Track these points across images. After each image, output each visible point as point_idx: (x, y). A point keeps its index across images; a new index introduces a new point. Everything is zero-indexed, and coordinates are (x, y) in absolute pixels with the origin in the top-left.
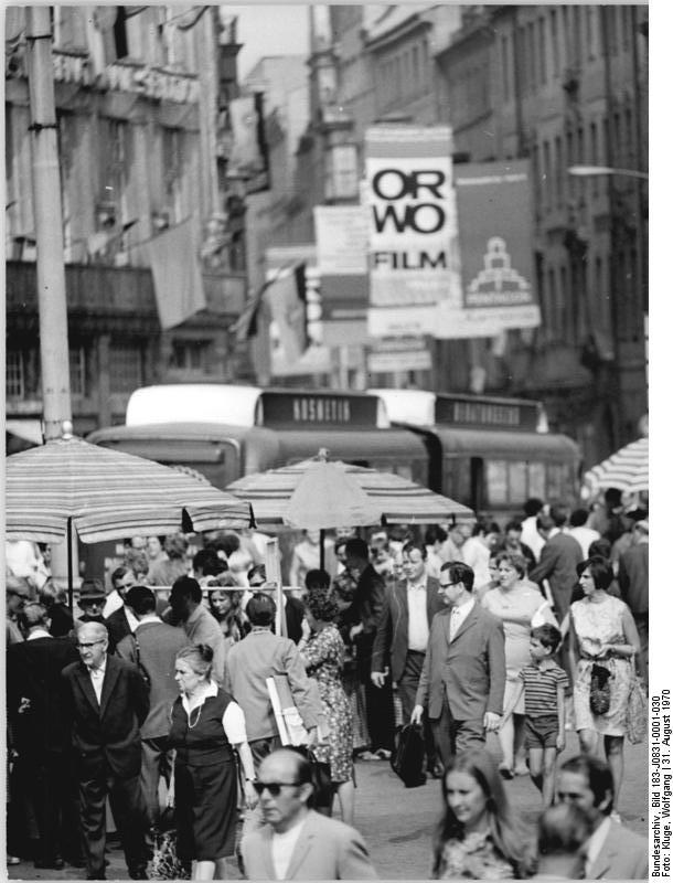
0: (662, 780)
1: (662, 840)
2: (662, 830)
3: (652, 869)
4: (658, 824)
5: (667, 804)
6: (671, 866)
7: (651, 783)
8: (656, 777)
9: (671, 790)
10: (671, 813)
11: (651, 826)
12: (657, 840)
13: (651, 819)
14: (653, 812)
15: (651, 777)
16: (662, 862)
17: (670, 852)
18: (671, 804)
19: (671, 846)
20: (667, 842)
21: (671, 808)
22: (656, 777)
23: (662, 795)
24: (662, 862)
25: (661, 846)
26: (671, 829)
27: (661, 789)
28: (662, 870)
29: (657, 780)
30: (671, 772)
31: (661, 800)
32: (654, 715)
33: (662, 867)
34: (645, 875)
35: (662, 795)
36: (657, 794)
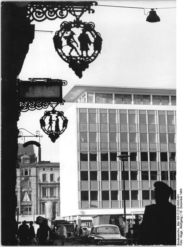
0: (180, 218)
1: (180, 235)
2: (180, 232)
3: (177, 243)
4: (179, 230)
5: (181, 225)
6: (182, 242)
7: (177, 219)
9: (182, 221)
10: (182, 227)
11: (177, 231)
12: (179, 235)
13: (177, 229)
14: (177, 227)
15: (177, 218)
16: (180, 241)
19: (182, 237)
20: (181, 235)
21: (182, 226)
23: (180, 222)
24: (180, 241)
25: (180, 237)
27: (180, 221)
29: (178, 218)
30: (182, 216)
33: (180, 243)
34: (176, 245)
35: (180, 222)
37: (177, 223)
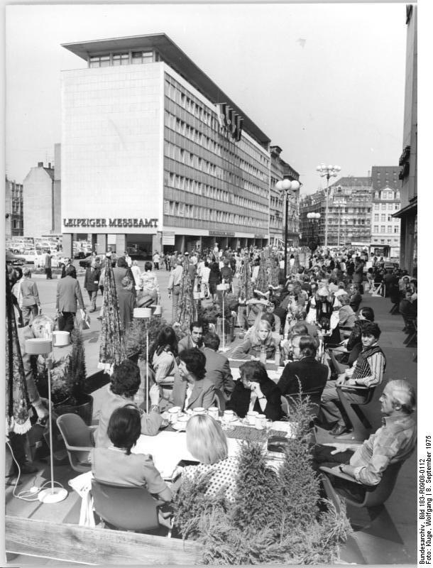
0: (426, 502)
1: (426, 540)
2: (426, 534)
4: (423, 530)
5: (429, 517)
6: (432, 557)
8: (422, 500)
9: (432, 508)
10: (432, 523)
11: (419, 531)
12: (423, 540)
13: (419, 527)
14: (420, 523)
15: (419, 500)
16: (426, 554)
17: (431, 548)
18: (432, 517)
19: (432, 544)
20: (429, 541)
21: (432, 520)
22: (422, 500)
23: (426, 511)
24: (426, 554)
25: (426, 544)
26: (432, 534)
27: (425, 507)
28: (426, 559)
29: (423, 502)
30: (432, 497)
31: (426, 514)
32: (421, 474)
33: (426, 558)
35: (426, 511)
36: (423, 511)
37: (419, 512)
